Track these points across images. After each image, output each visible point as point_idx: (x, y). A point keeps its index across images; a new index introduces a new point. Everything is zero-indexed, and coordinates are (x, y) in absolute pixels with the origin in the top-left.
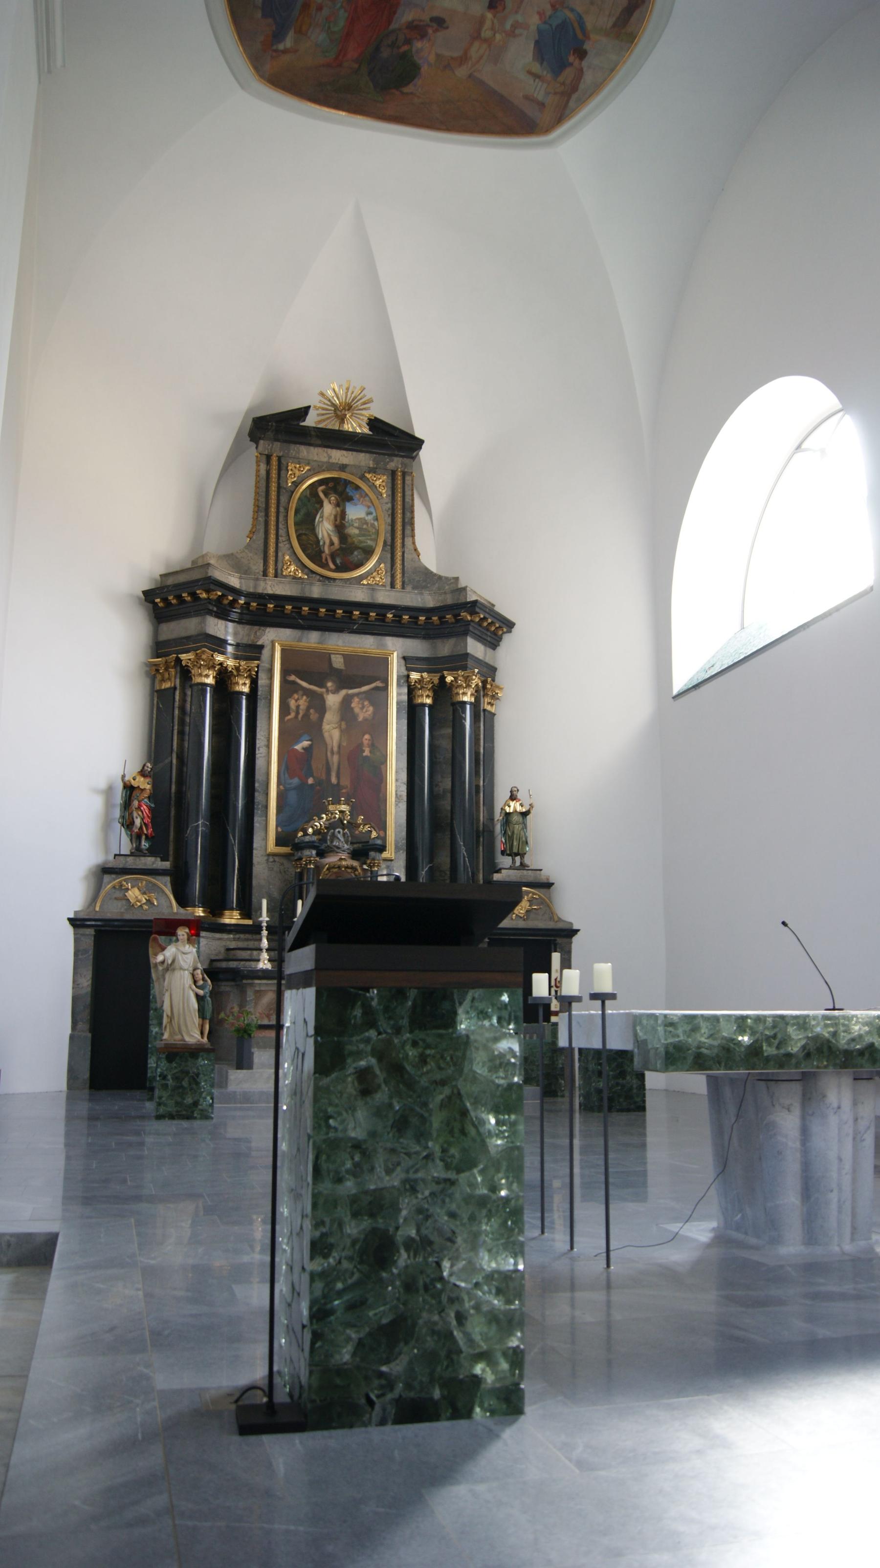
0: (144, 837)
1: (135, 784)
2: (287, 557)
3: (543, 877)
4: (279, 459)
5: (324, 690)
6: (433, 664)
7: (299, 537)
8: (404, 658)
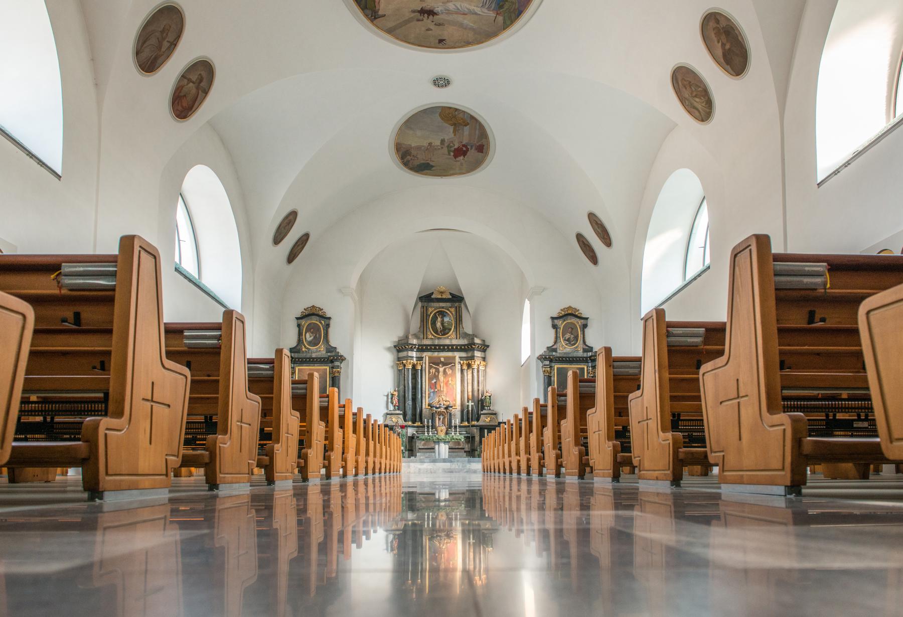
6: (467, 358)
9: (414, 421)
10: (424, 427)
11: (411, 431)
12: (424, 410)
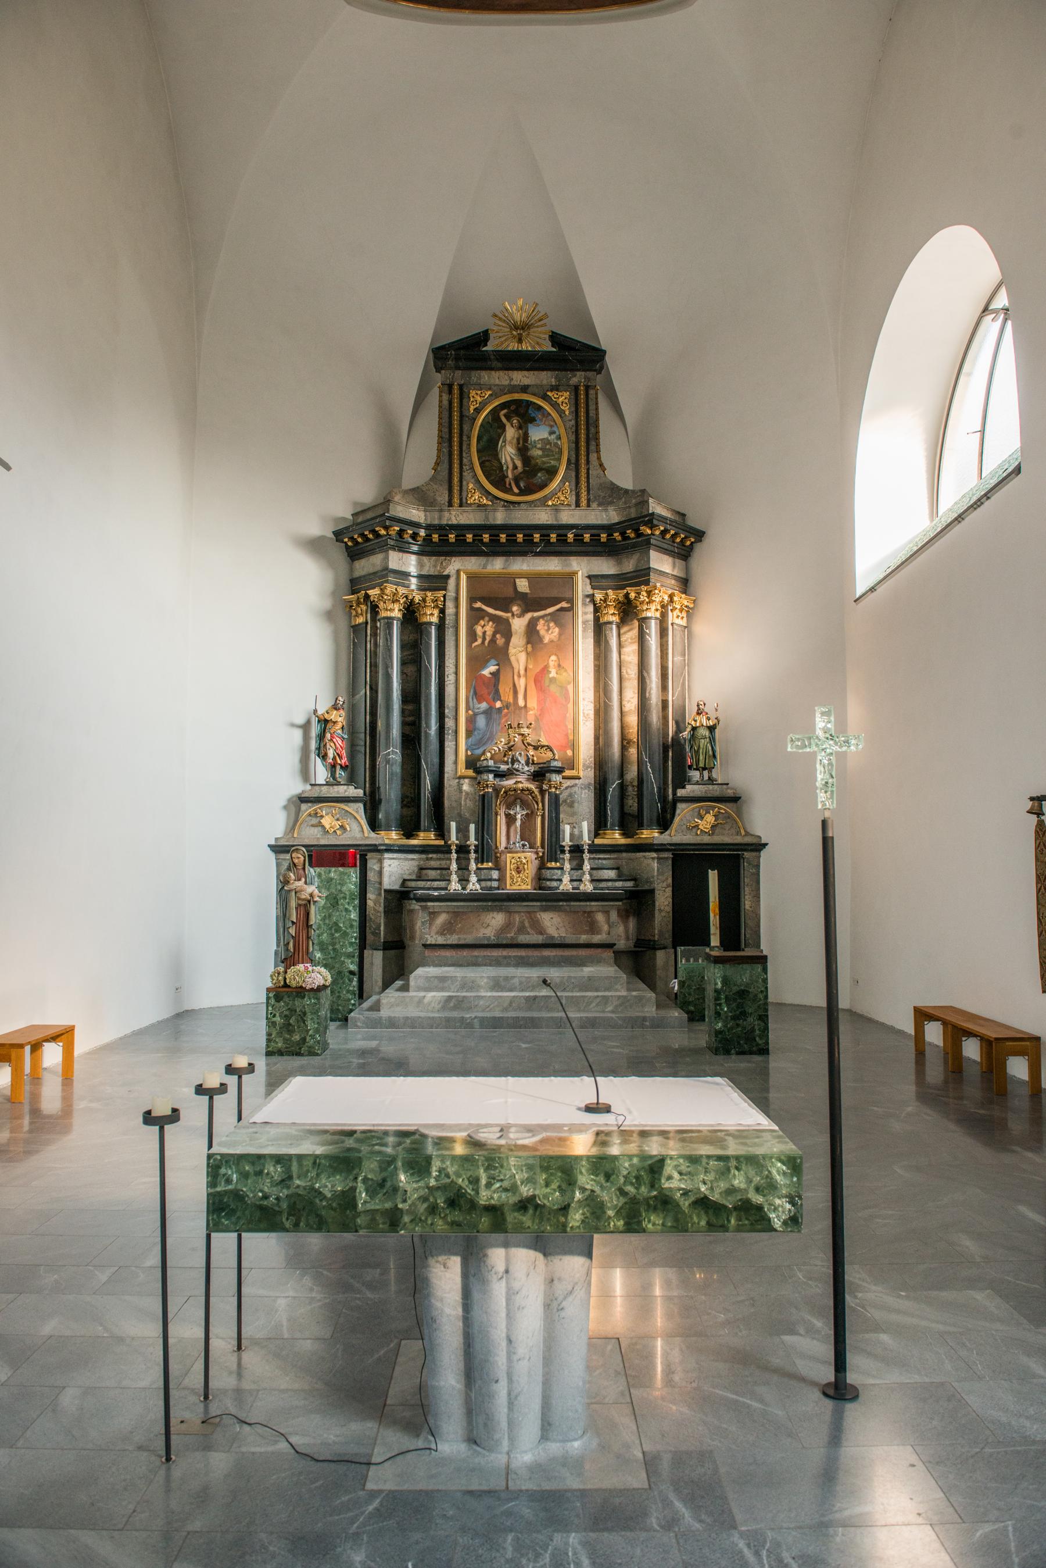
0: (338, 767)
1: (326, 716)
2: (471, 486)
3: (730, 793)
4: (461, 387)
5: (509, 615)
6: (621, 581)
7: (482, 464)
8: (589, 577)
9: (409, 829)
10: (446, 850)
11: (393, 870)
12: (449, 783)
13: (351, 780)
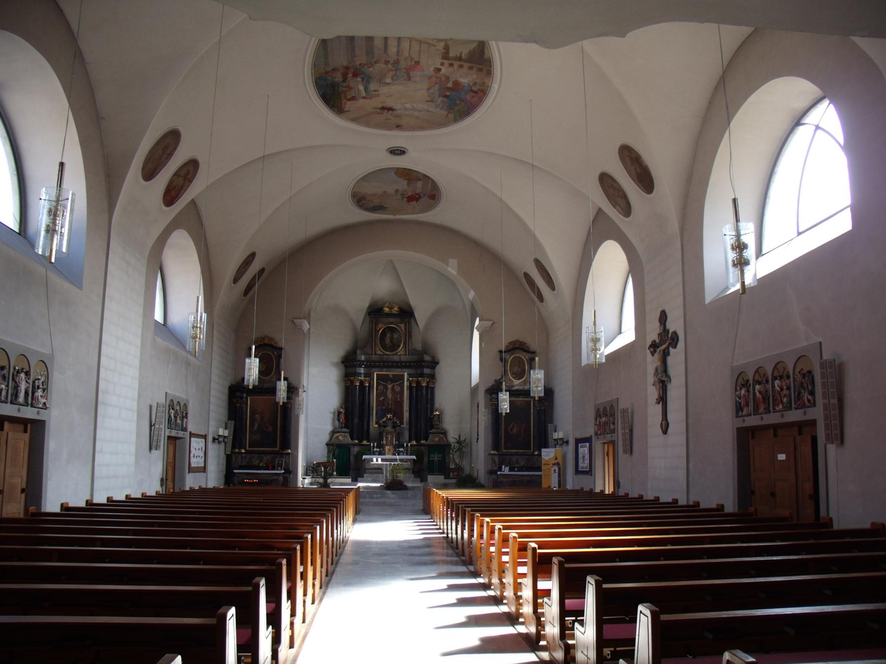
13: (345, 427)
